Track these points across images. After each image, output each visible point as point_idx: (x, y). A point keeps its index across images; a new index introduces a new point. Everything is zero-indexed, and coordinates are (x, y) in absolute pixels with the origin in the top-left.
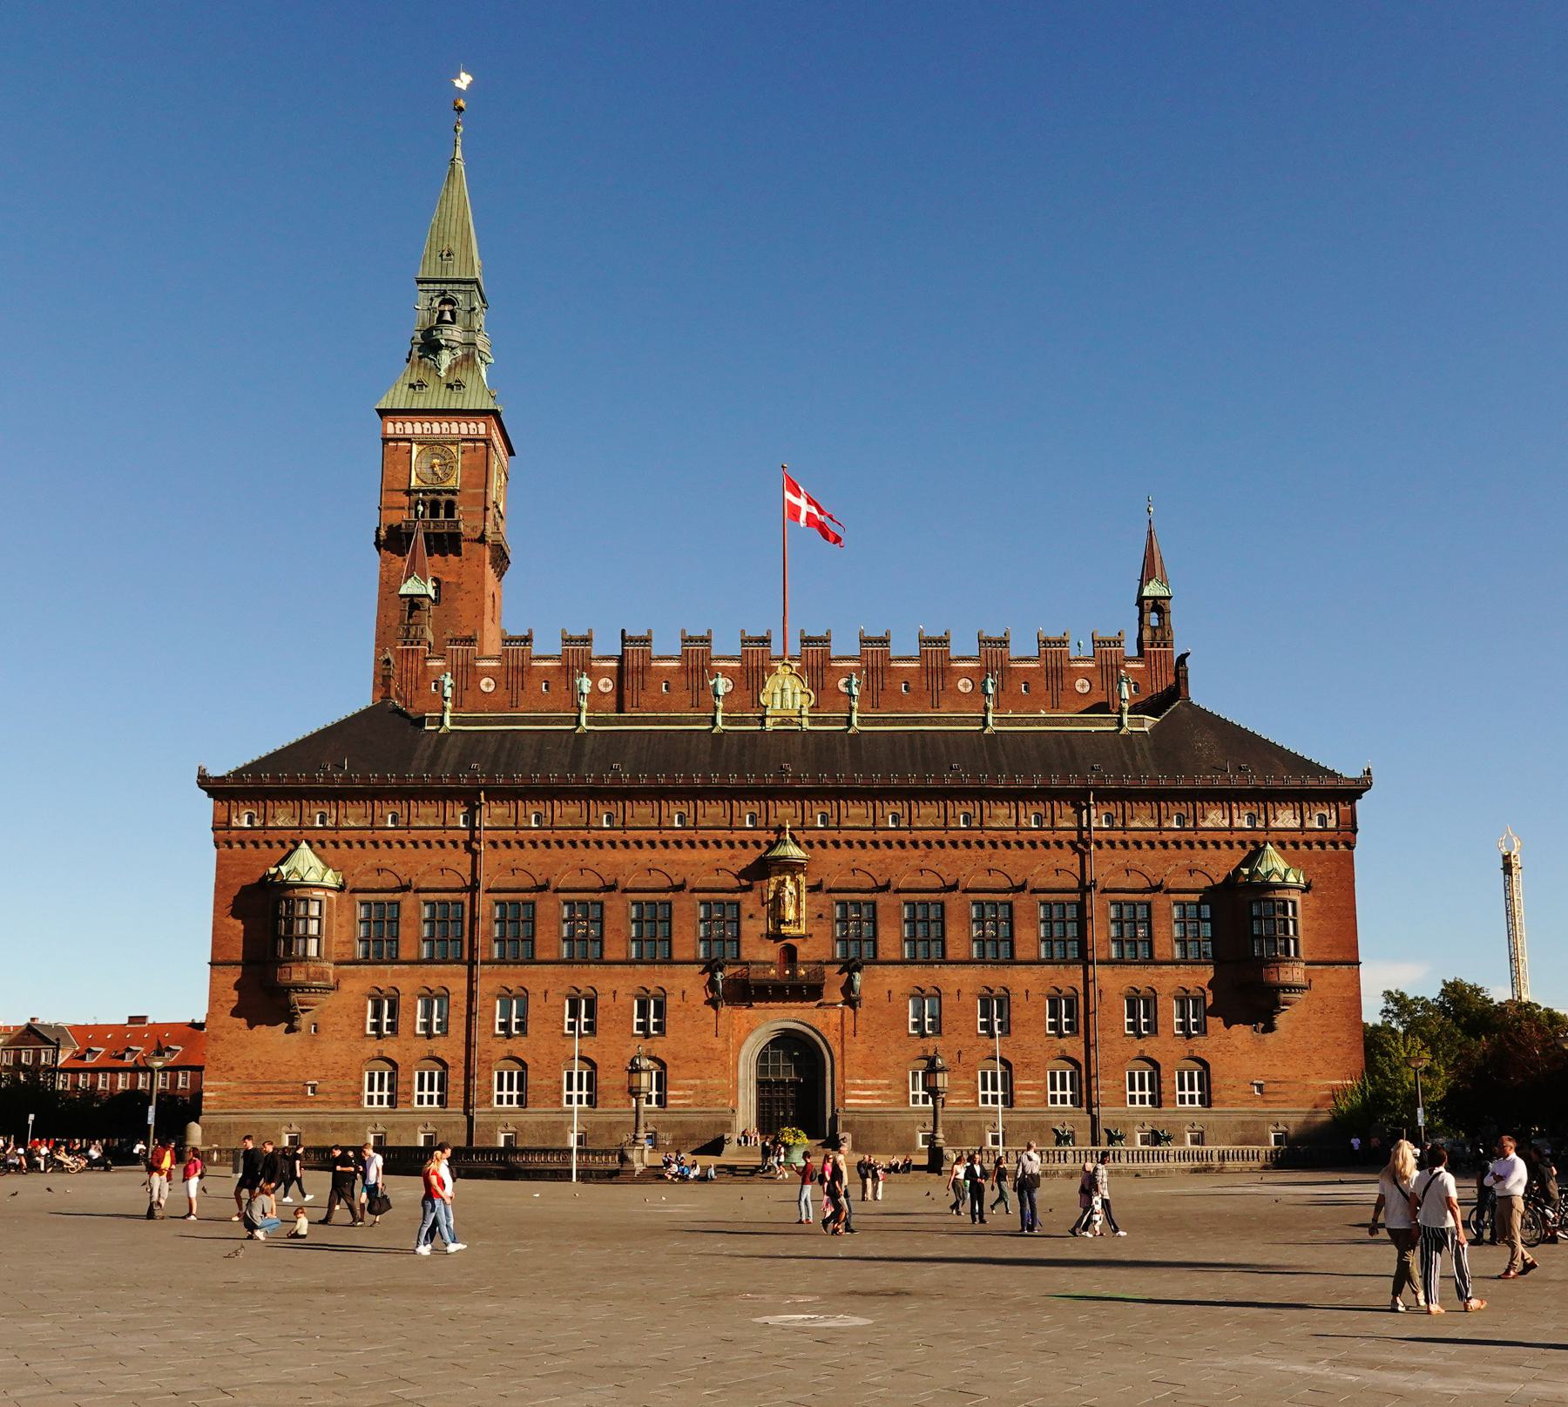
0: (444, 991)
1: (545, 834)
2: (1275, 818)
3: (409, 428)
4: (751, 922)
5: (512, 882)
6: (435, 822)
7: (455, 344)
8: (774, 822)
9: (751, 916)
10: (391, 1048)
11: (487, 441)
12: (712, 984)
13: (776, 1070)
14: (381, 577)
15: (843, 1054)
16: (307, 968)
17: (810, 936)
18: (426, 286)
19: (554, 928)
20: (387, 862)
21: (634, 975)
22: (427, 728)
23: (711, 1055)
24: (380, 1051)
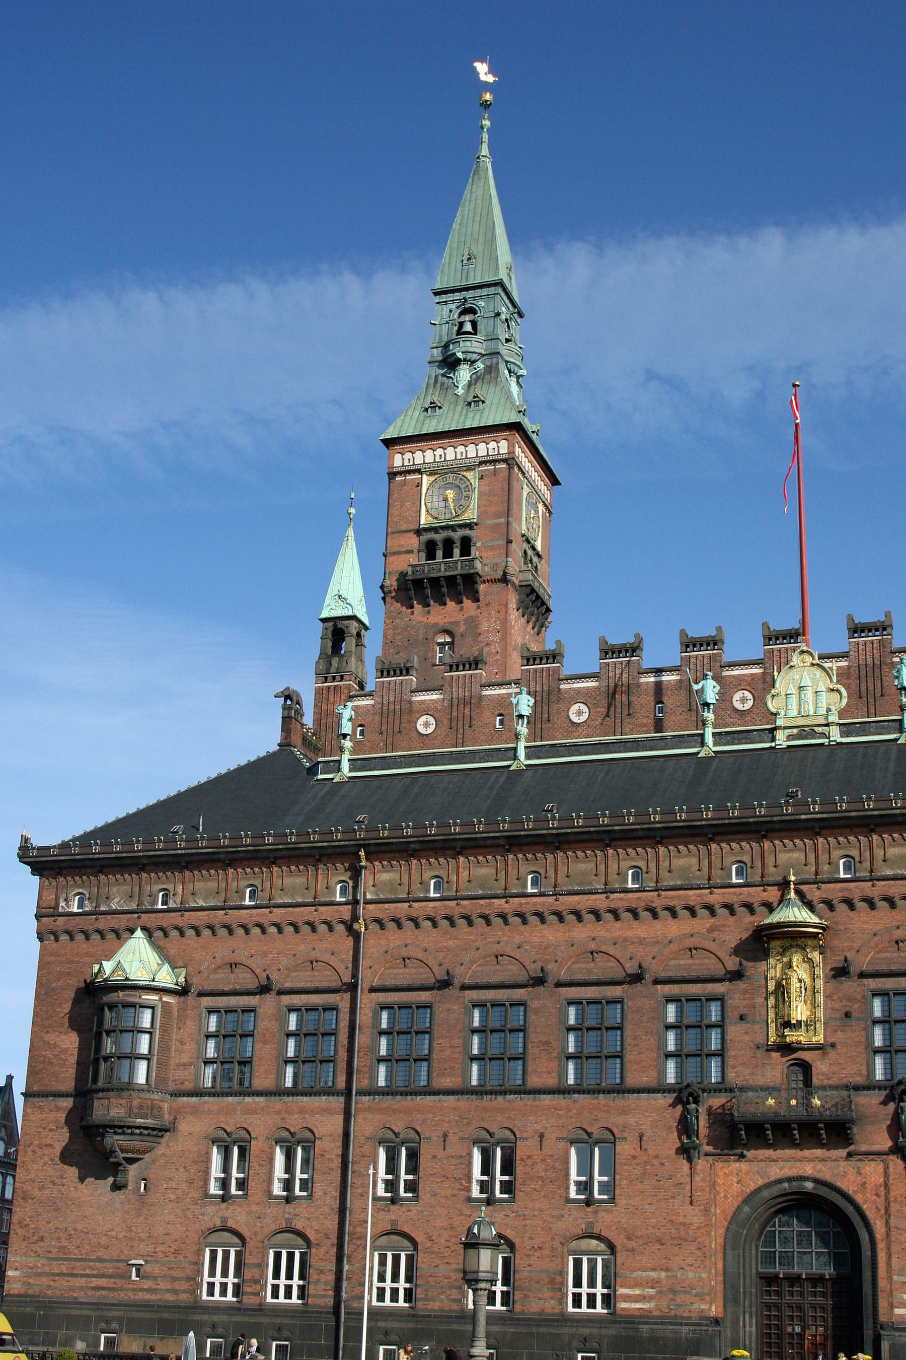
0: (308, 1134)
1: (446, 907)
3: (419, 458)
4: (742, 1027)
5: (403, 976)
6: (303, 896)
7: (475, 357)
8: (774, 874)
9: (742, 1018)
10: (238, 1217)
11: (510, 461)
12: (685, 1127)
13: (786, 1259)
14: (385, 637)
15: (888, 1235)
16: (130, 1098)
17: (833, 1045)
18: (444, 298)
19: (458, 1042)
20: (241, 956)
21: (569, 1110)
22: (320, 777)
23: (683, 1234)
24: (224, 1219)
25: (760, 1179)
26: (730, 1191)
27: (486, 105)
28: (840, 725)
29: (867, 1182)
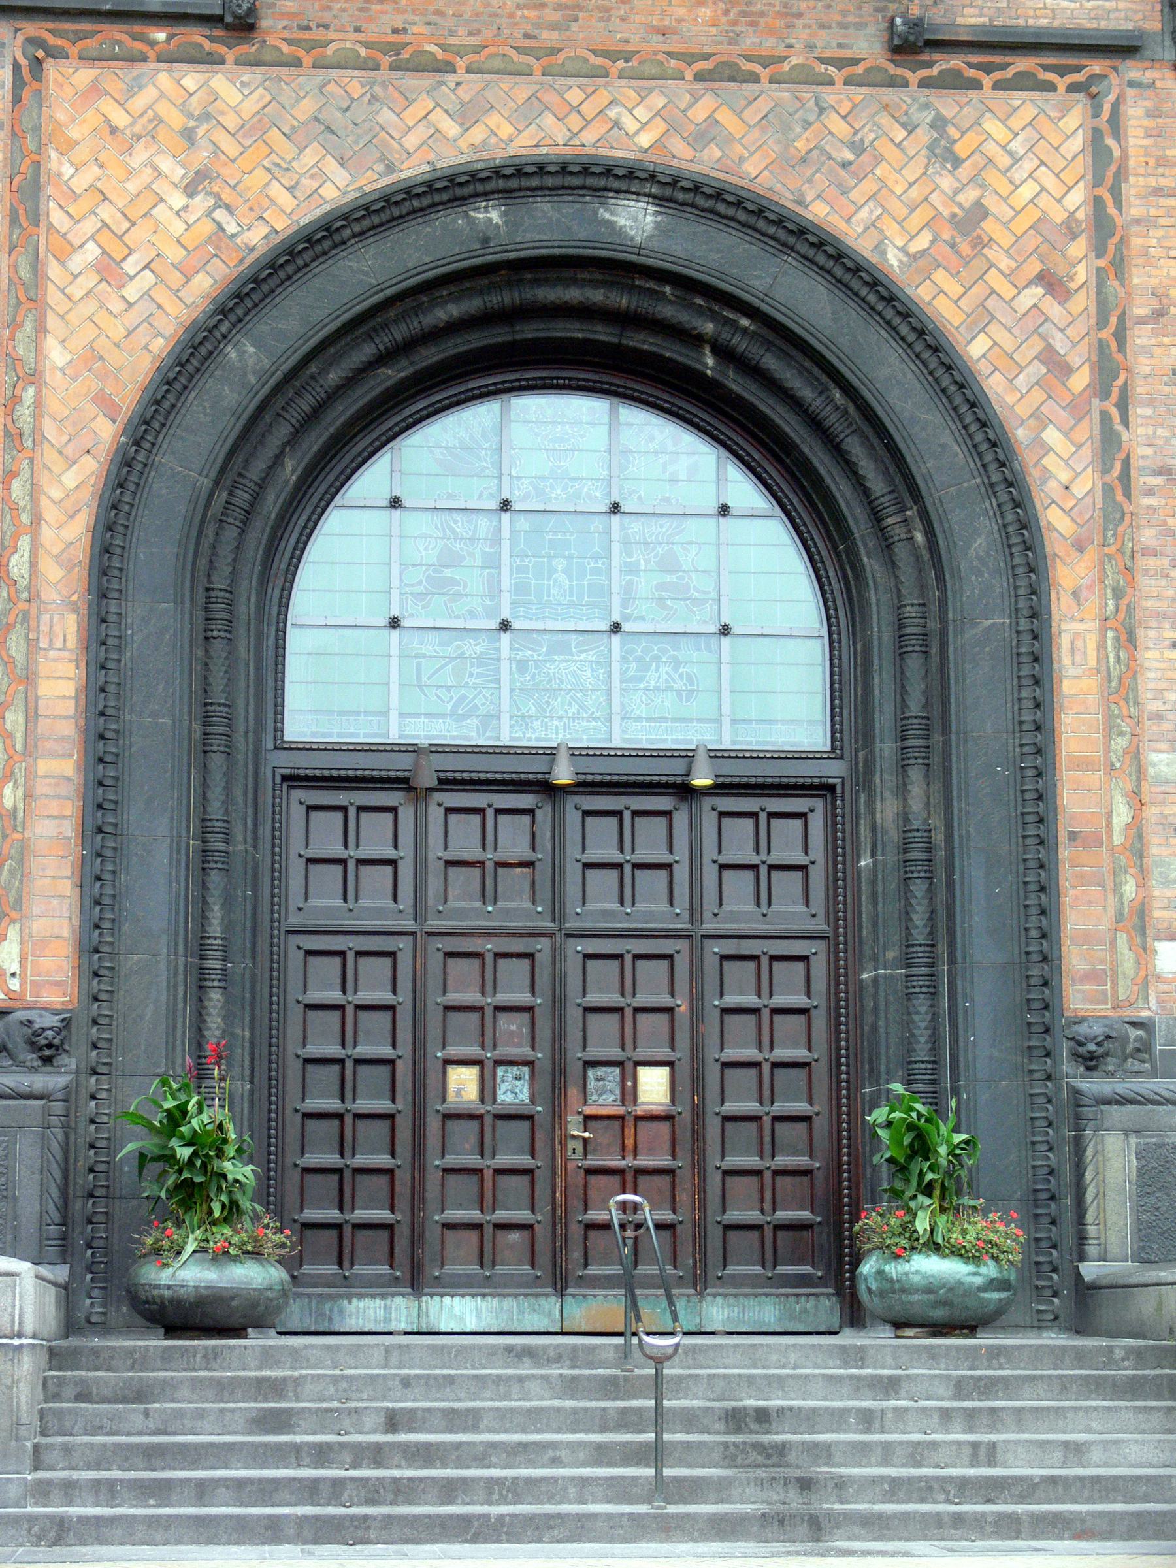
25: (331, 166)
26: (136, 236)
29: (990, 202)
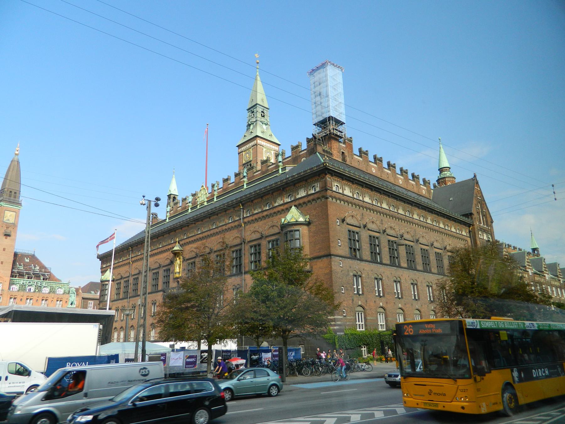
2: (298, 194)
7: (253, 122)
27: (258, 63)
28: (207, 201)
